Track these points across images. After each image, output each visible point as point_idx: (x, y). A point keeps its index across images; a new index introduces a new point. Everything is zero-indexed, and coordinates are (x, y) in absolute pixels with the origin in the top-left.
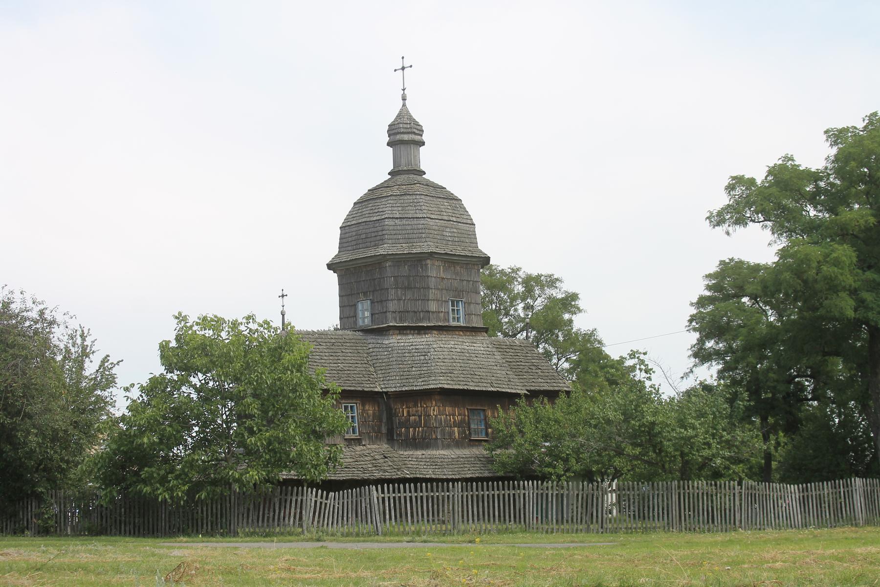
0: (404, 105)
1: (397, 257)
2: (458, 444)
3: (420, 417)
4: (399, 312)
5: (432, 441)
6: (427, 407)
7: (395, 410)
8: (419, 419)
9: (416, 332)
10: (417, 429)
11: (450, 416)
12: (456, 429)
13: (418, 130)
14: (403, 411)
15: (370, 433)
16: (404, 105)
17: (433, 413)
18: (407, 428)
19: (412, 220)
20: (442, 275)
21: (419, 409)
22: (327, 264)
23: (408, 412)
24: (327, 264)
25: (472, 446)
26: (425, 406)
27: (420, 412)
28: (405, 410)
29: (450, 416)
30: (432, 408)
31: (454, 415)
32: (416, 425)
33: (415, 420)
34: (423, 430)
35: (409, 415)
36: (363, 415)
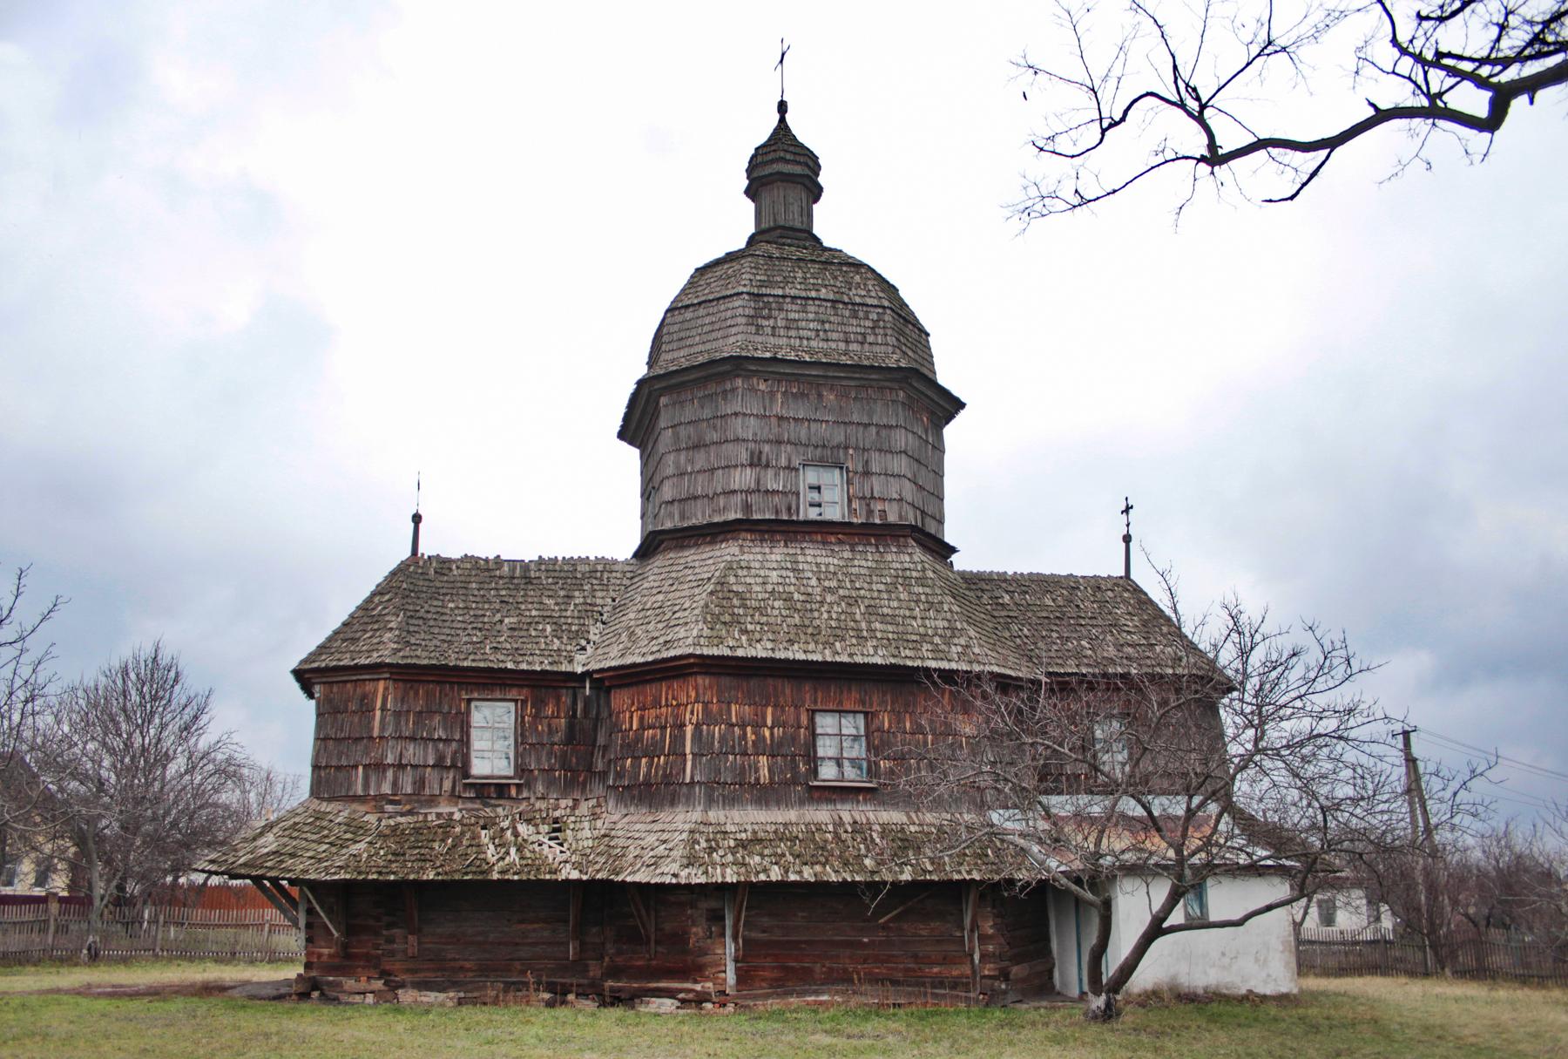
0: (782, 120)
1: (673, 381)
2: (765, 795)
3: (664, 728)
4: (680, 501)
5: (684, 789)
6: (678, 705)
7: (618, 717)
8: (661, 734)
9: (708, 539)
10: (656, 759)
11: (743, 726)
12: (763, 760)
13: (811, 163)
14: (631, 717)
15: (552, 770)
16: (782, 120)
17: (690, 719)
18: (637, 759)
19: (715, 303)
20: (778, 408)
21: (664, 710)
22: (622, 435)
23: (641, 719)
24: (622, 435)
25: (819, 801)
26: (674, 703)
27: (663, 718)
28: (635, 714)
29: (743, 726)
30: (689, 707)
31: (758, 725)
32: (652, 752)
33: (654, 736)
34: (666, 763)
35: (642, 727)
36: (534, 724)
